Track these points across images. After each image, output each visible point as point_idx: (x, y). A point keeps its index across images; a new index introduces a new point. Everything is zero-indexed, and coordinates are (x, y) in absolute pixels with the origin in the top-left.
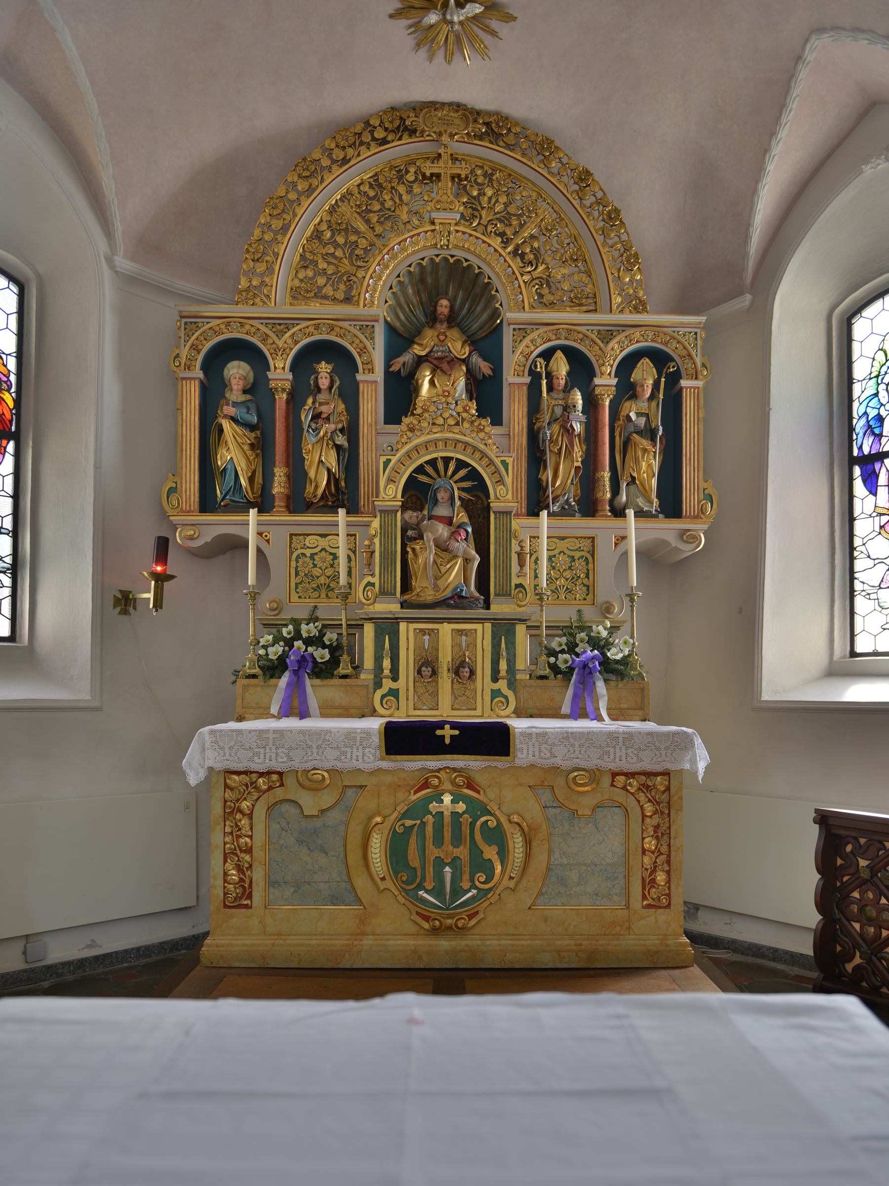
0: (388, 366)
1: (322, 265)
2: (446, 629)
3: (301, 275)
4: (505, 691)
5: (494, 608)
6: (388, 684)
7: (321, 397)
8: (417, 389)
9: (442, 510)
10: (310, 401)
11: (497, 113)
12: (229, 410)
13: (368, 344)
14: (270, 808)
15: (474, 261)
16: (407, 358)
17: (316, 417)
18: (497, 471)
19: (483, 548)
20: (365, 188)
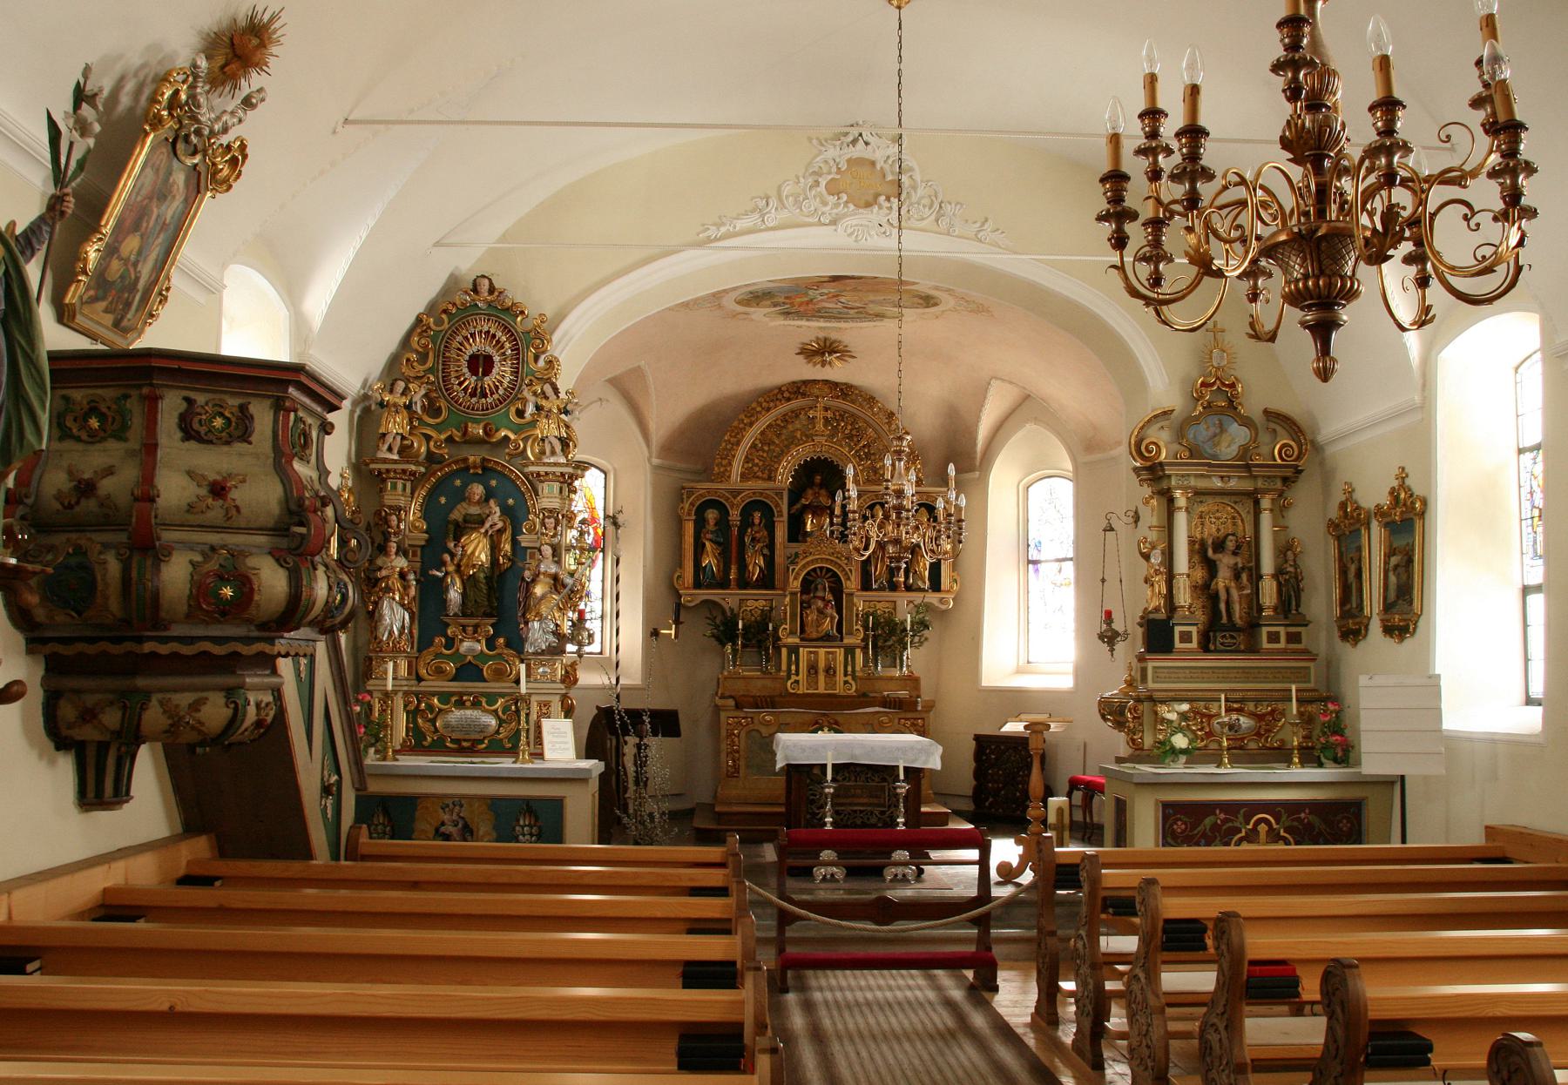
0: (789, 511)
1: (756, 461)
2: (822, 651)
3: (746, 466)
4: (851, 681)
5: (845, 641)
6: (794, 678)
7: (756, 528)
8: (805, 524)
9: (820, 594)
10: (749, 530)
11: (846, 384)
12: (709, 536)
13: (780, 502)
14: (749, 732)
15: (834, 459)
16: (798, 506)
17: (753, 539)
18: (847, 574)
19: (840, 612)
20: (779, 422)
